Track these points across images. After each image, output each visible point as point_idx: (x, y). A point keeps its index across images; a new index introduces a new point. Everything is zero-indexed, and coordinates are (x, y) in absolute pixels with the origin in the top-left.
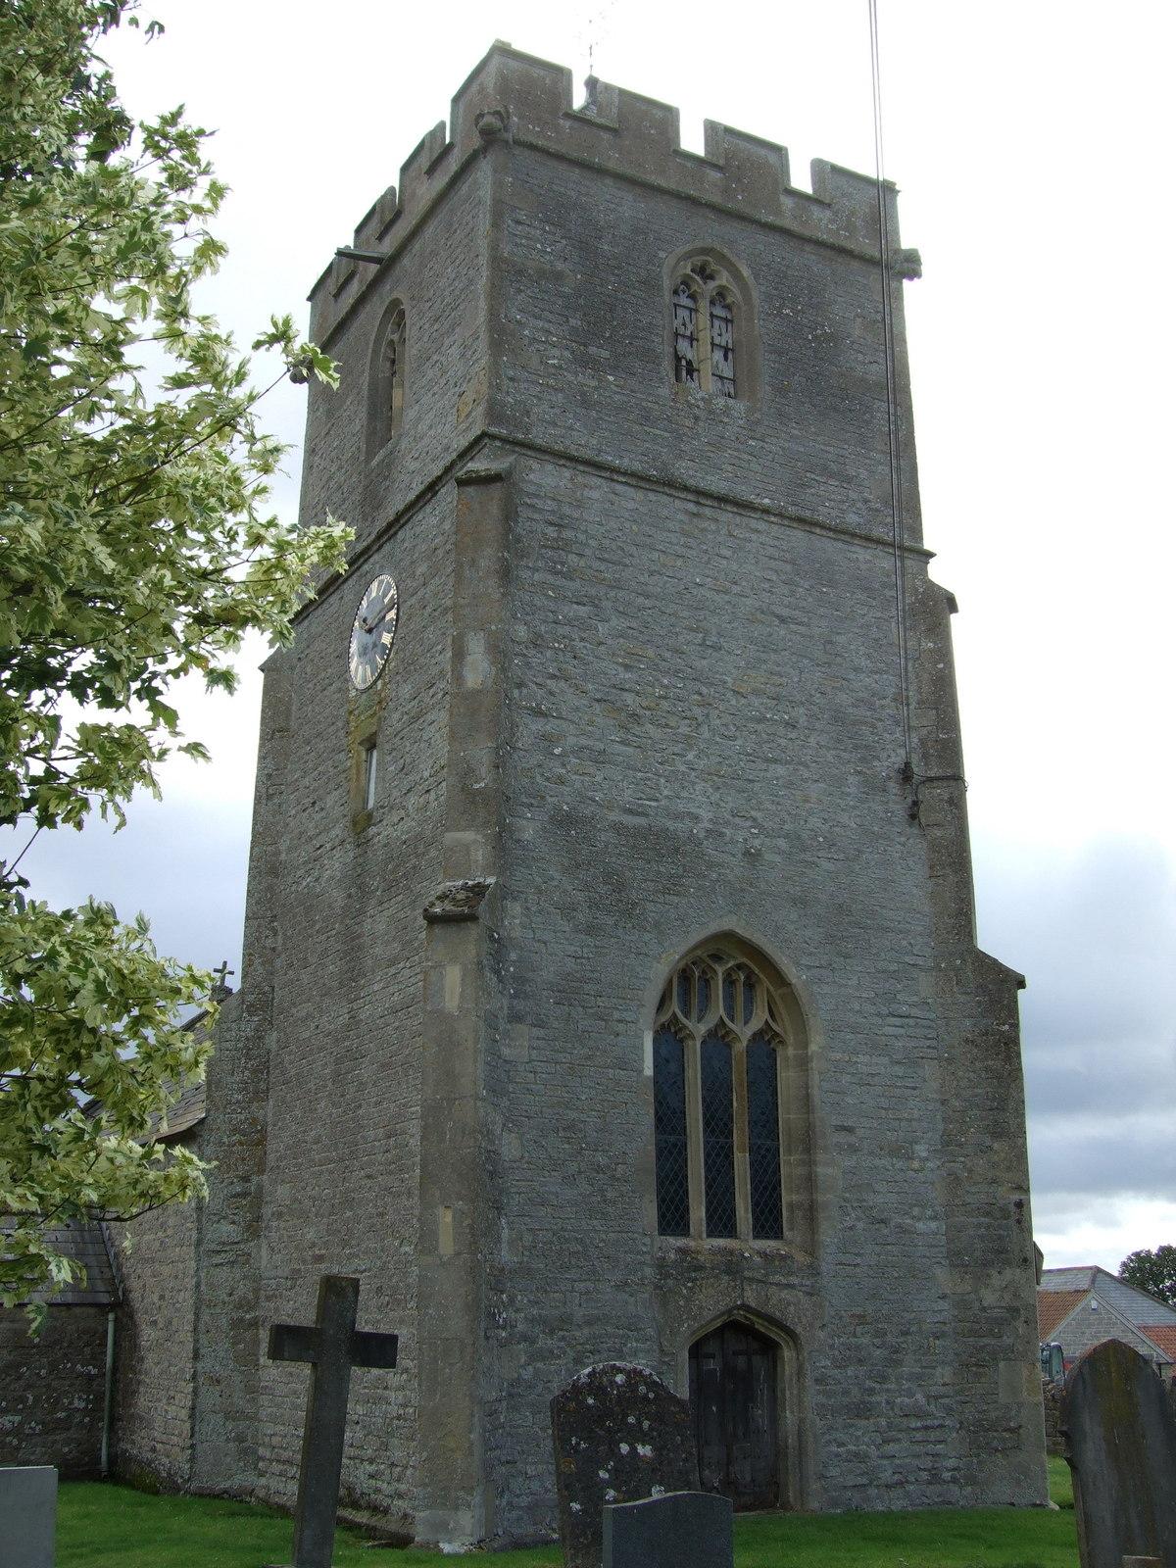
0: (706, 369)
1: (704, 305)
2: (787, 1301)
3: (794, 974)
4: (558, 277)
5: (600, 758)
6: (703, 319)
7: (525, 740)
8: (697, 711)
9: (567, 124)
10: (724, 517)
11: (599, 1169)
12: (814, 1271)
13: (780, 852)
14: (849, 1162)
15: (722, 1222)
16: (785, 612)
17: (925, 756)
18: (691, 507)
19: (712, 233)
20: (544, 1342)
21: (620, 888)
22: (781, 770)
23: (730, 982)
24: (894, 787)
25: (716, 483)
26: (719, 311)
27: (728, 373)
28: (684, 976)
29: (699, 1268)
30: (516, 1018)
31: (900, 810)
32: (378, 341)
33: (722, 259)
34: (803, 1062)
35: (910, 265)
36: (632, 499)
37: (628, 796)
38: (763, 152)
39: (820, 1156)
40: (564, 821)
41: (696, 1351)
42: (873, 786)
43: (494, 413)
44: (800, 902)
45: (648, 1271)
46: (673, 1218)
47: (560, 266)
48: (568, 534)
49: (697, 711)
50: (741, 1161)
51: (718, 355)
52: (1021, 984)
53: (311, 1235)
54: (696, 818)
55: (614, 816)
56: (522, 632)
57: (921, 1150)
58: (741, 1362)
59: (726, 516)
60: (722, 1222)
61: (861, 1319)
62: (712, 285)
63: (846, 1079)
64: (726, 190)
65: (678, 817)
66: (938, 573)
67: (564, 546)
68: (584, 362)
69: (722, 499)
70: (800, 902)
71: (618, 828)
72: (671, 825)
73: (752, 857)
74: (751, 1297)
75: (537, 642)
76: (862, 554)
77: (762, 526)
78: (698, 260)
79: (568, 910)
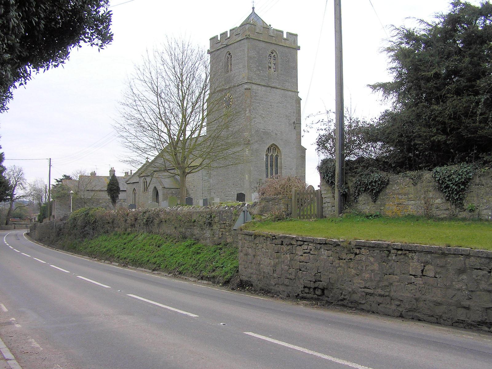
0: (272, 67)
1: (272, 58)
3: (281, 149)
4: (255, 57)
5: (260, 123)
8: (271, 116)
11: (260, 171)
14: (285, 170)
16: (281, 102)
17: (296, 121)
19: (273, 47)
22: (280, 123)
24: (293, 124)
26: (274, 58)
28: (268, 148)
31: (293, 128)
32: (225, 56)
34: (281, 159)
35: (299, 48)
36: (264, 88)
38: (280, 33)
39: (282, 170)
42: (290, 124)
43: (248, 79)
44: (282, 140)
46: (267, 176)
49: (271, 116)
52: (306, 149)
53: (221, 178)
54: (270, 130)
55: (261, 130)
57: (293, 169)
59: (275, 89)
62: (273, 54)
63: (286, 161)
64: (276, 40)
66: (300, 95)
67: (256, 96)
70: (282, 140)
71: (262, 131)
76: (290, 93)
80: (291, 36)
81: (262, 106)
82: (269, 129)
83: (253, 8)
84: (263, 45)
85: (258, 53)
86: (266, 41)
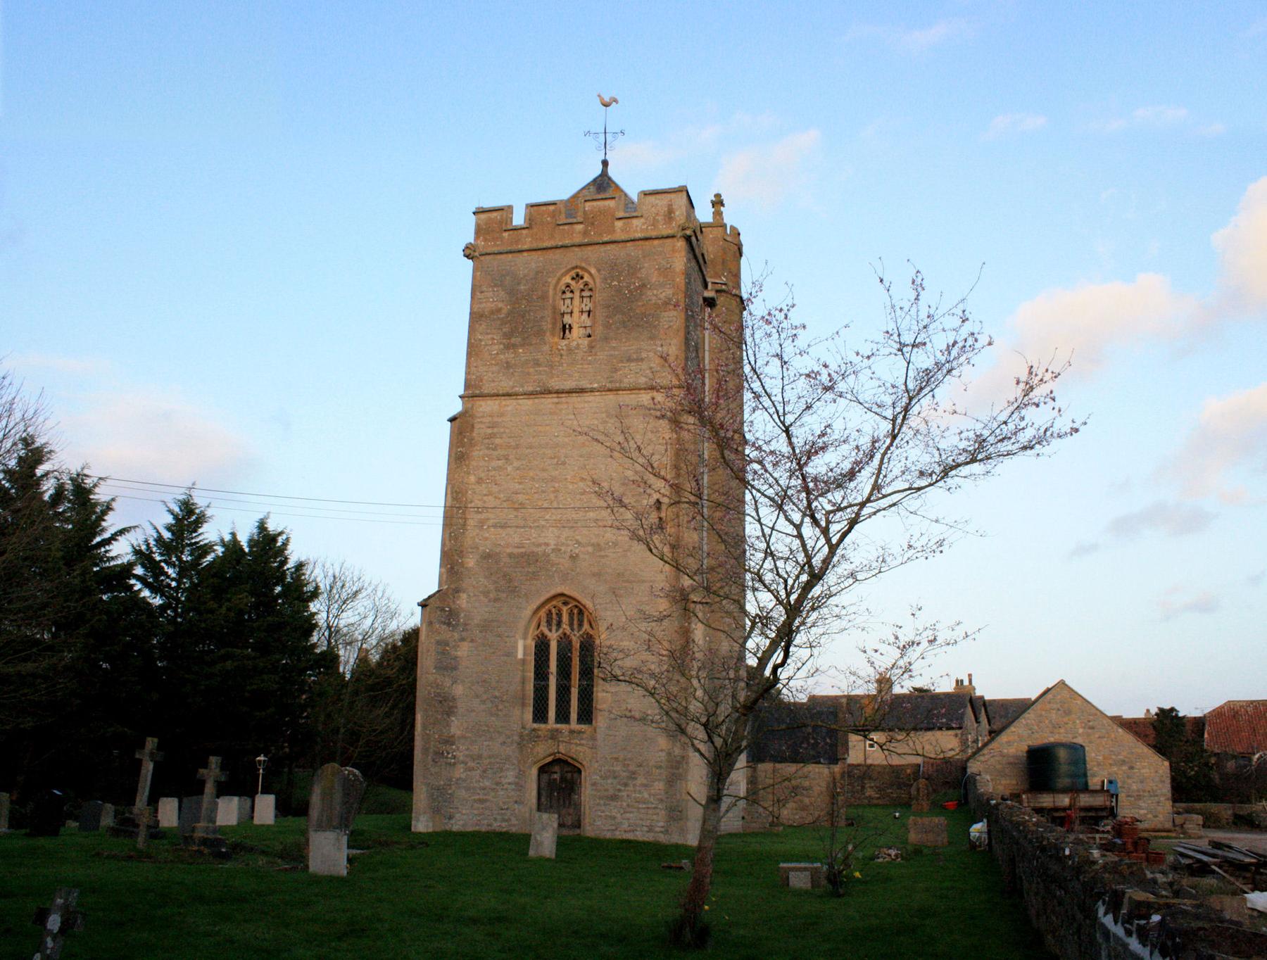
0: (575, 326)
2: (578, 750)
4: (499, 310)
6: (577, 301)
7: (471, 522)
8: (552, 496)
9: (506, 235)
10: (569, 400)
12: (594, 738)
13: (588, 553)
15: (563, 716)
18: (556, 400)
19: (574, 257)
20: (471, 764)
21: (510, 581)
23: (571, 614)
25: (569, 385)
27: (589, 323)
29: (538, 737)
30: (463, 639)
33: (583, 269)
36: (527, 404)
37: (517, 540)
40: (487, 556)
41: (543, 770)
44: (597, 575)
45: (516, 738)
47: (500, 305)
48: (495, 430)
50: (575, 692)
51: (585, 316)
54: (547, 544)
55: (508, 551)
56: (472, 479)
58: (569, 775)
59: (574, 399)
60: (563, 716)
61: (616, 759)
65: (540, 545)
68: (508, 347)
69: (570, 392)
70: (597, 575)
71: (510, 555)
72: (535, 549)
73: (574, 558)
74: (562, 749)
75: (480, 481)
77: (591, 398)
78: (573, 273)
79: (486, 594)
80: (652, 198)
81: (516, 464)
82: (541, 540)
83: (605, 163)
84: (535, 261)
85: (511, 292)
86: (545, 245)
